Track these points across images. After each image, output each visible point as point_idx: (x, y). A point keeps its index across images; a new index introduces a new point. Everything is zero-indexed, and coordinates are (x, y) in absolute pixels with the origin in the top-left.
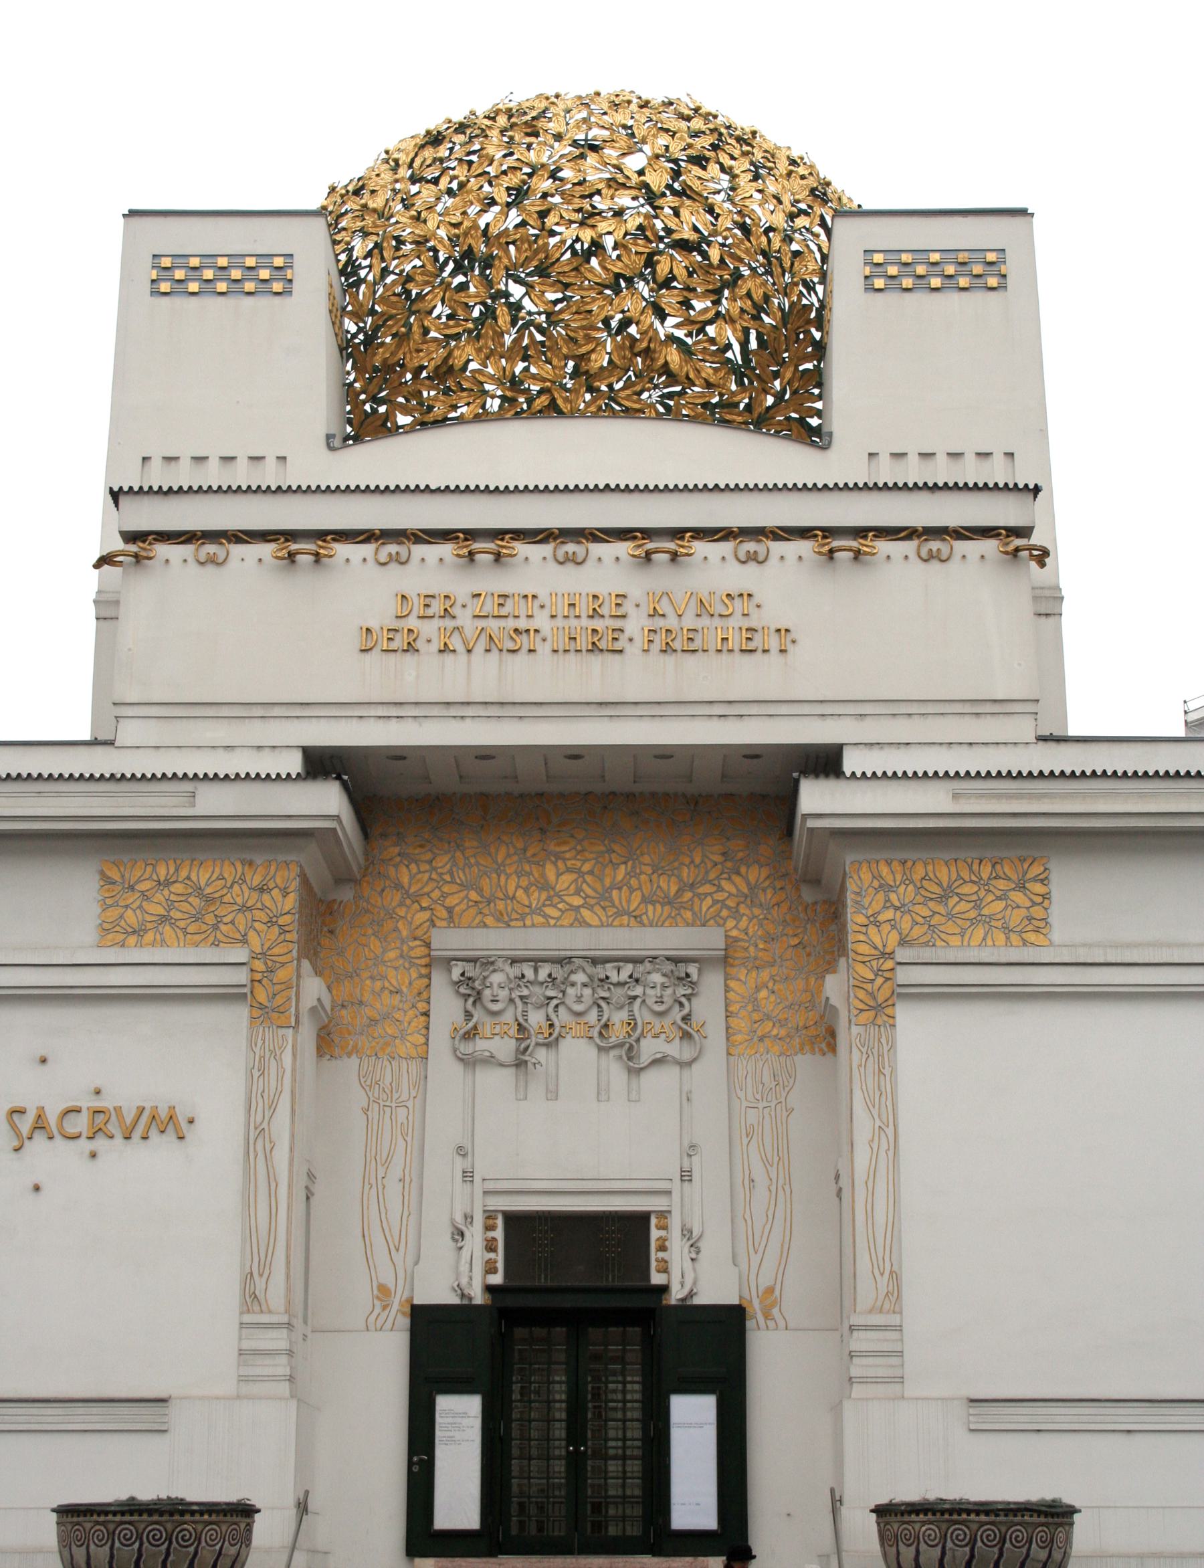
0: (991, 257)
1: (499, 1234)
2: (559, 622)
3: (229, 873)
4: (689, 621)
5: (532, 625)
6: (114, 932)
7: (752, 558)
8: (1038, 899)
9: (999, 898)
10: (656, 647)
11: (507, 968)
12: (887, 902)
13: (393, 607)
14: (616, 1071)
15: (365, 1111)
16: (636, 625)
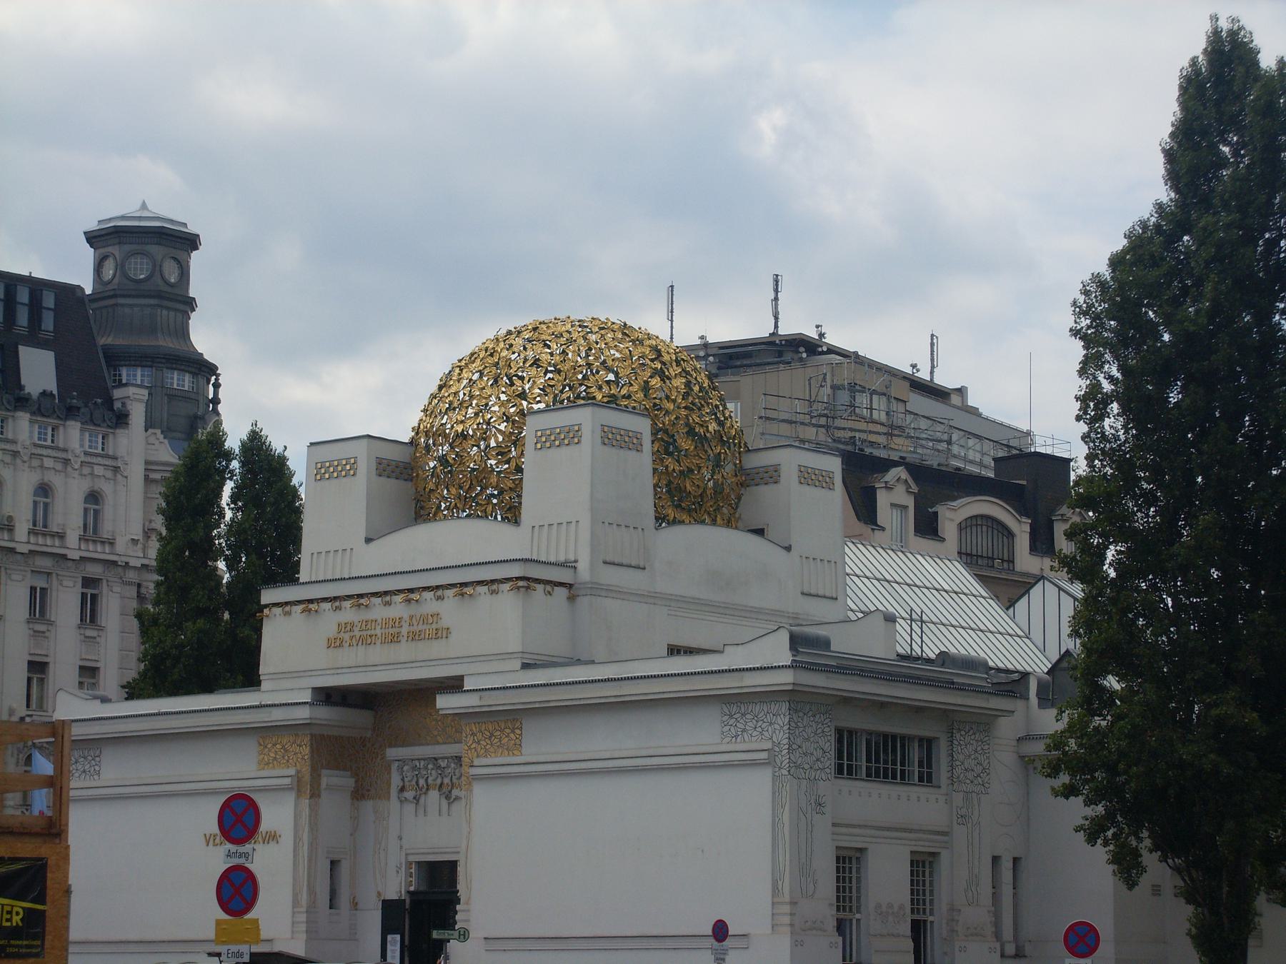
0: (576, 428)
1: (413, 871)
2: (383, 631)
3: (292, 739)
4: (421, 627)
5: (373, 632)
6: (264, 764)
7: (440, 598)
8: (518, 736)
9: (506, 736)
10: (410, 638)
11: (410, 763)
12: (474, 741)
13: (335, 628)
14: (444, 802)
15: (374, 822)
16: (404, 631)
